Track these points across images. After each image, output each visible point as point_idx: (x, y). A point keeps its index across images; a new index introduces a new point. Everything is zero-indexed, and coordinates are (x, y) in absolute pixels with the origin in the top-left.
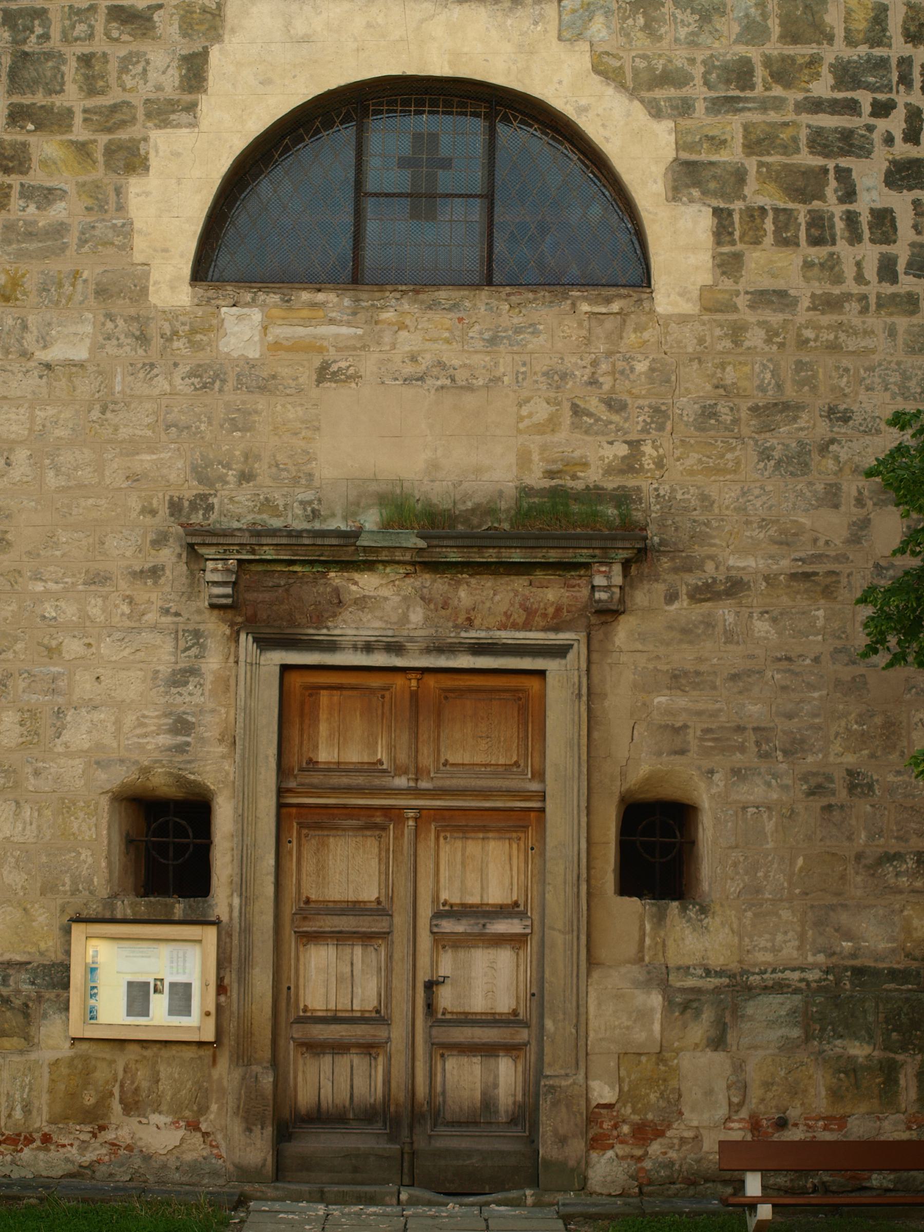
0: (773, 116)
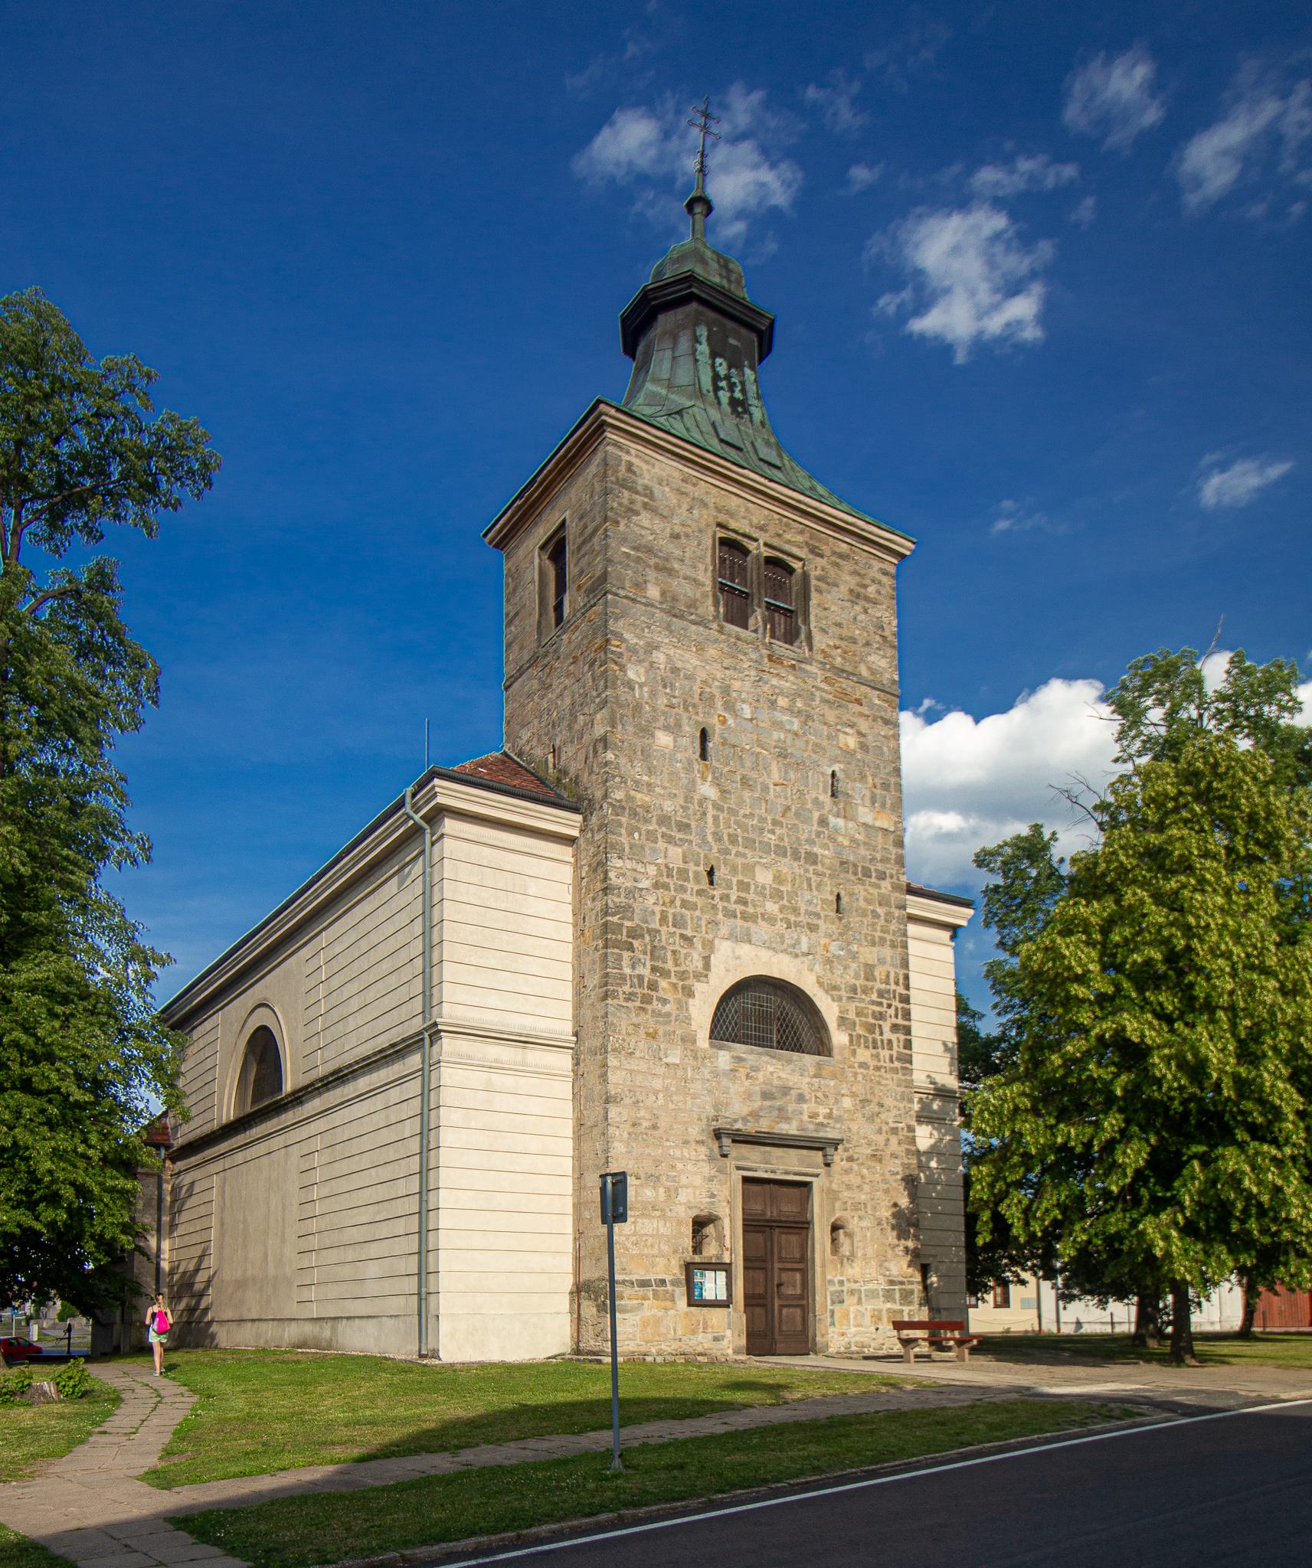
0: (863, 1005)
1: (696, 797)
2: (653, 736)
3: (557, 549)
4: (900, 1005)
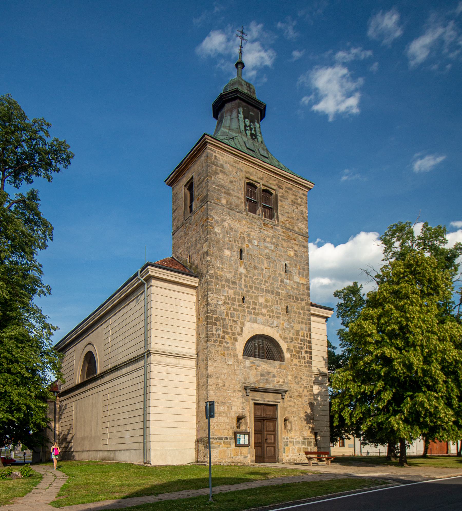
1: (238, 273)
2: (223, 251)
3: (190, 186)
4: (308, 344)
